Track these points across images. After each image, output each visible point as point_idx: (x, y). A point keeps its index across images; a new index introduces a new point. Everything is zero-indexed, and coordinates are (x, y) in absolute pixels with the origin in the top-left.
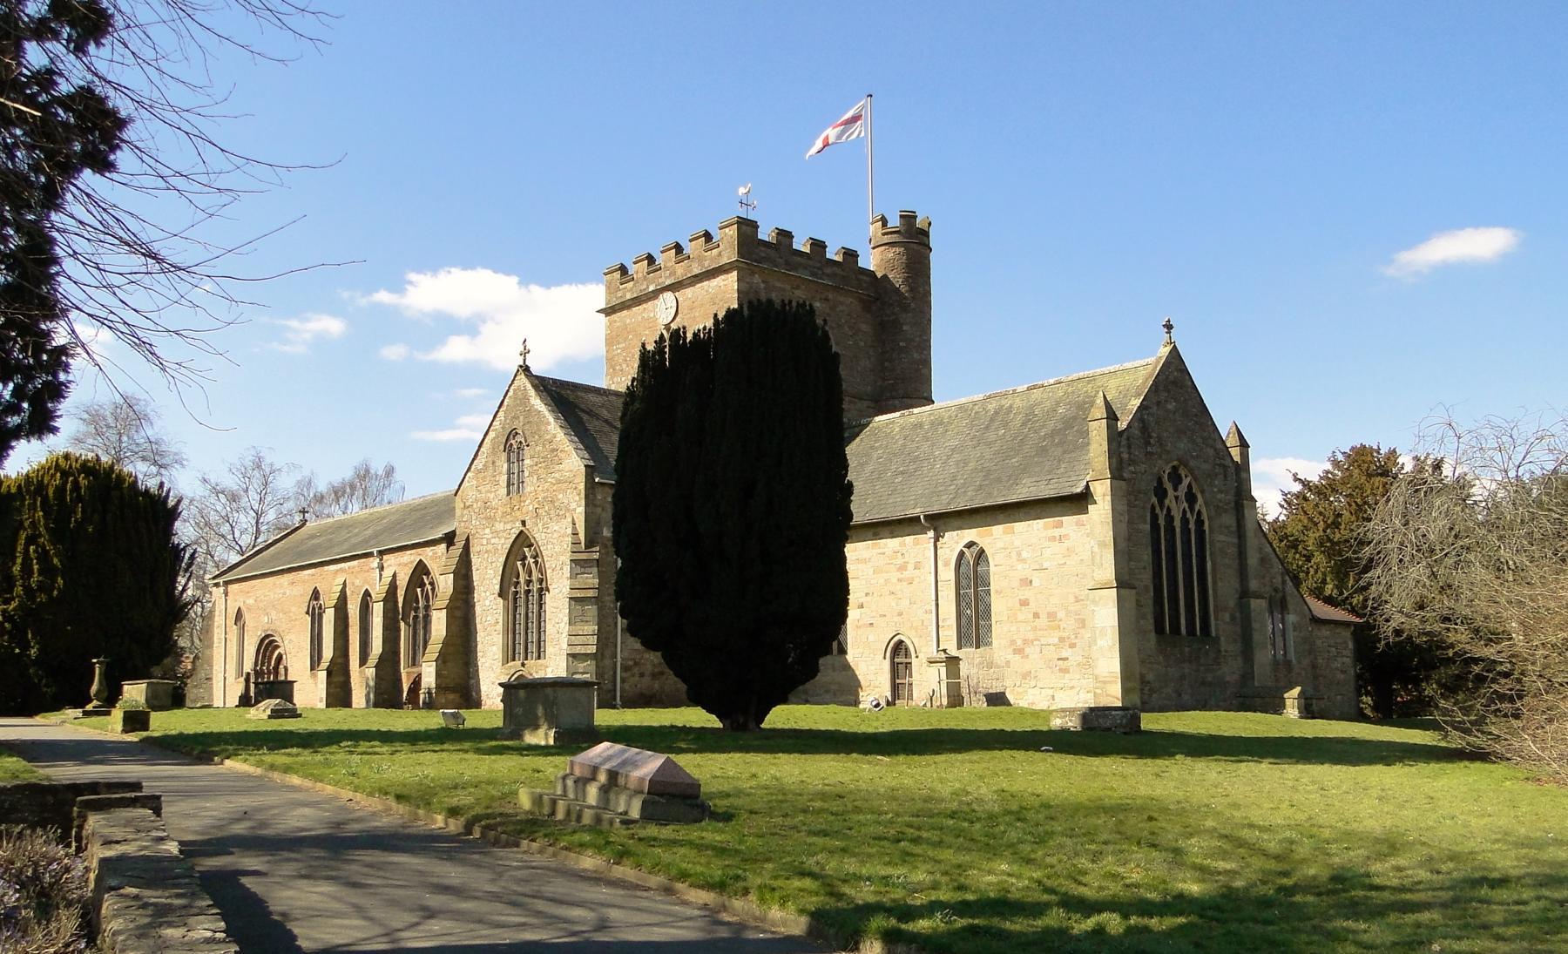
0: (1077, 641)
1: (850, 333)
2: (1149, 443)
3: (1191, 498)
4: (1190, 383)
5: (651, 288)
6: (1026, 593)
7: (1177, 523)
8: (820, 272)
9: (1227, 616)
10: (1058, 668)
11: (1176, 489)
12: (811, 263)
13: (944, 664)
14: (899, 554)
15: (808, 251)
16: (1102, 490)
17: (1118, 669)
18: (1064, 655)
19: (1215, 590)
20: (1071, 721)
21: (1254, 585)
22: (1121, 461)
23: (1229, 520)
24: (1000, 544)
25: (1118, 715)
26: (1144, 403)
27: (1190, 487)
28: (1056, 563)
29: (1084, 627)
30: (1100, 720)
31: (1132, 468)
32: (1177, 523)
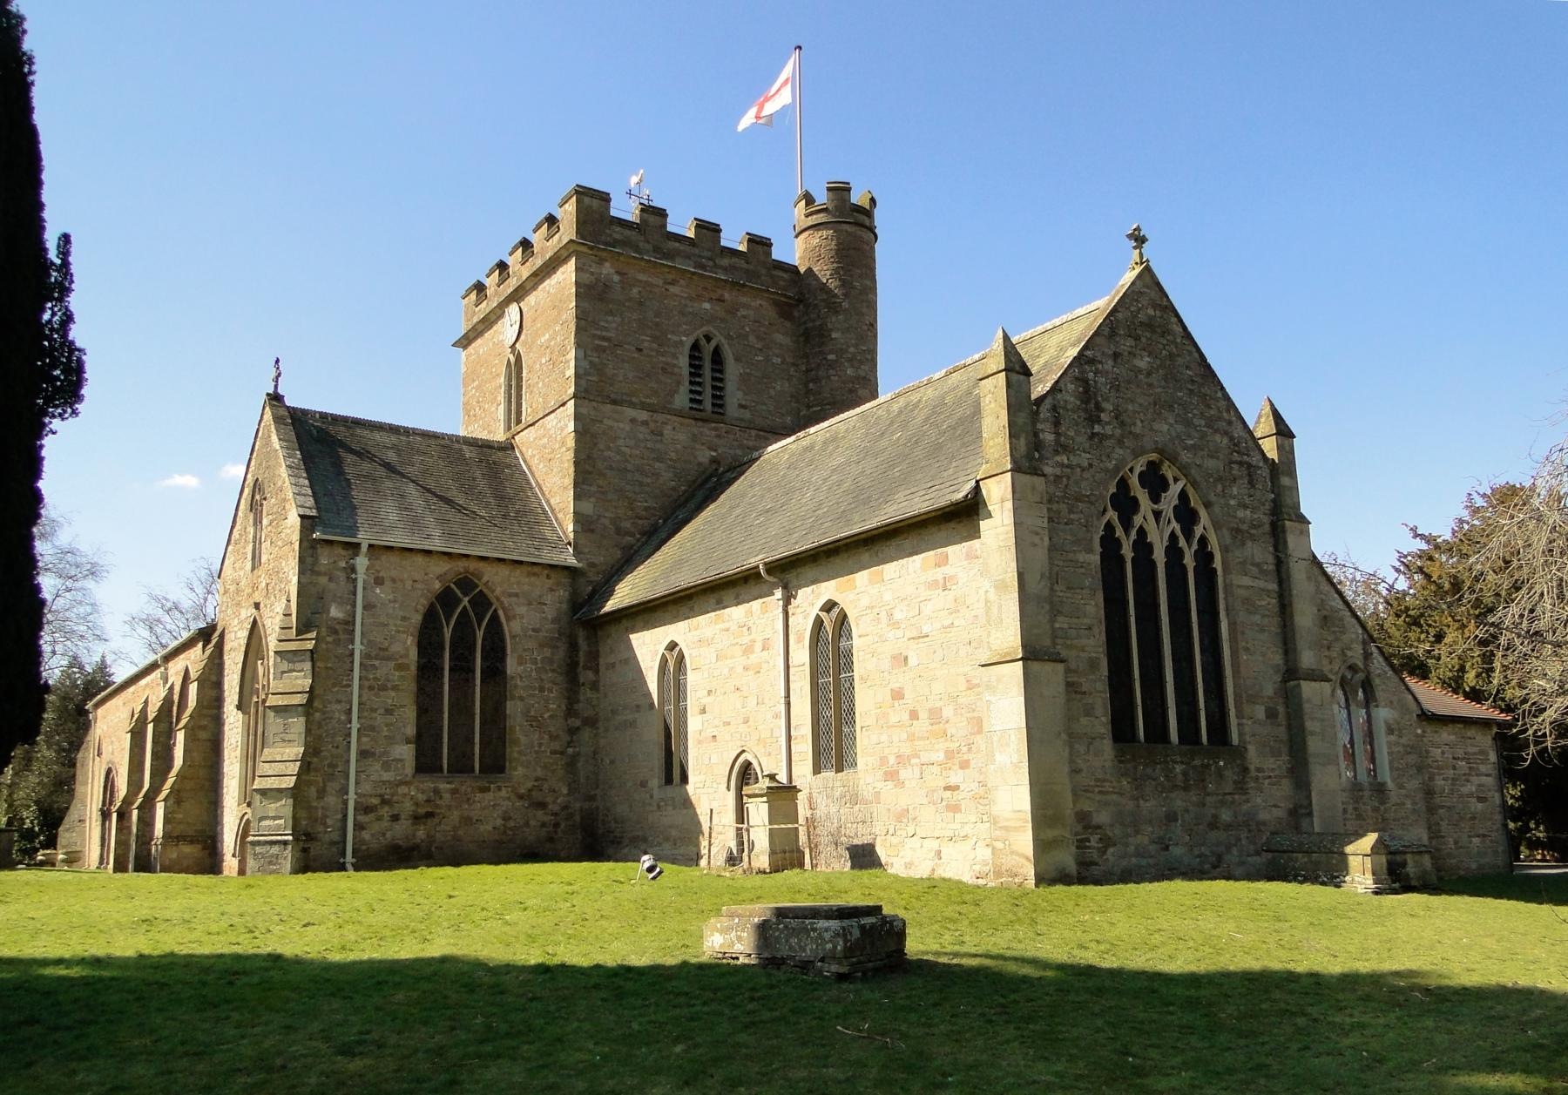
0: (970, 756)
1: (759, 346)
2: (1099, 421)
3: (1186, 515)
4: (1179, 329)
6: (899, 680)
7: (1159, 556)
8: (711, 263)
9: (1260, 712)
10: (944, 803)
11: (1155, 498)
12: (696, 251)
13: (765, 799)
14: (745, 629)
15: (693, 236)
16: (998, 493)
17: (1026, 805)
18: (953, 781)
19: (1236, 673)
20: (739, 939)
21: (1307, 659)
22: (1037, 445)
23: (1260, 552)
24: (865, 601)
25: (827, 930)
26: (1088, 353)
27: (1183, 496)
28: (938, 625)
29: (980, 731)
30: (794, 941)
31: (1064, 459)
32: (1159, 556)
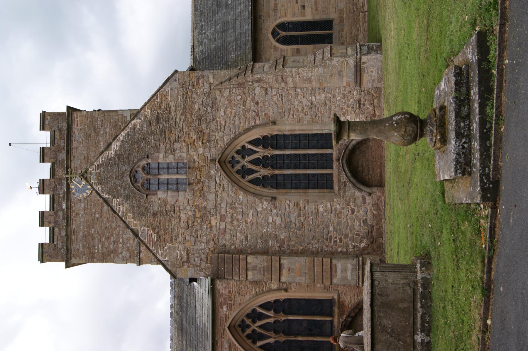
5: (64, 206)
